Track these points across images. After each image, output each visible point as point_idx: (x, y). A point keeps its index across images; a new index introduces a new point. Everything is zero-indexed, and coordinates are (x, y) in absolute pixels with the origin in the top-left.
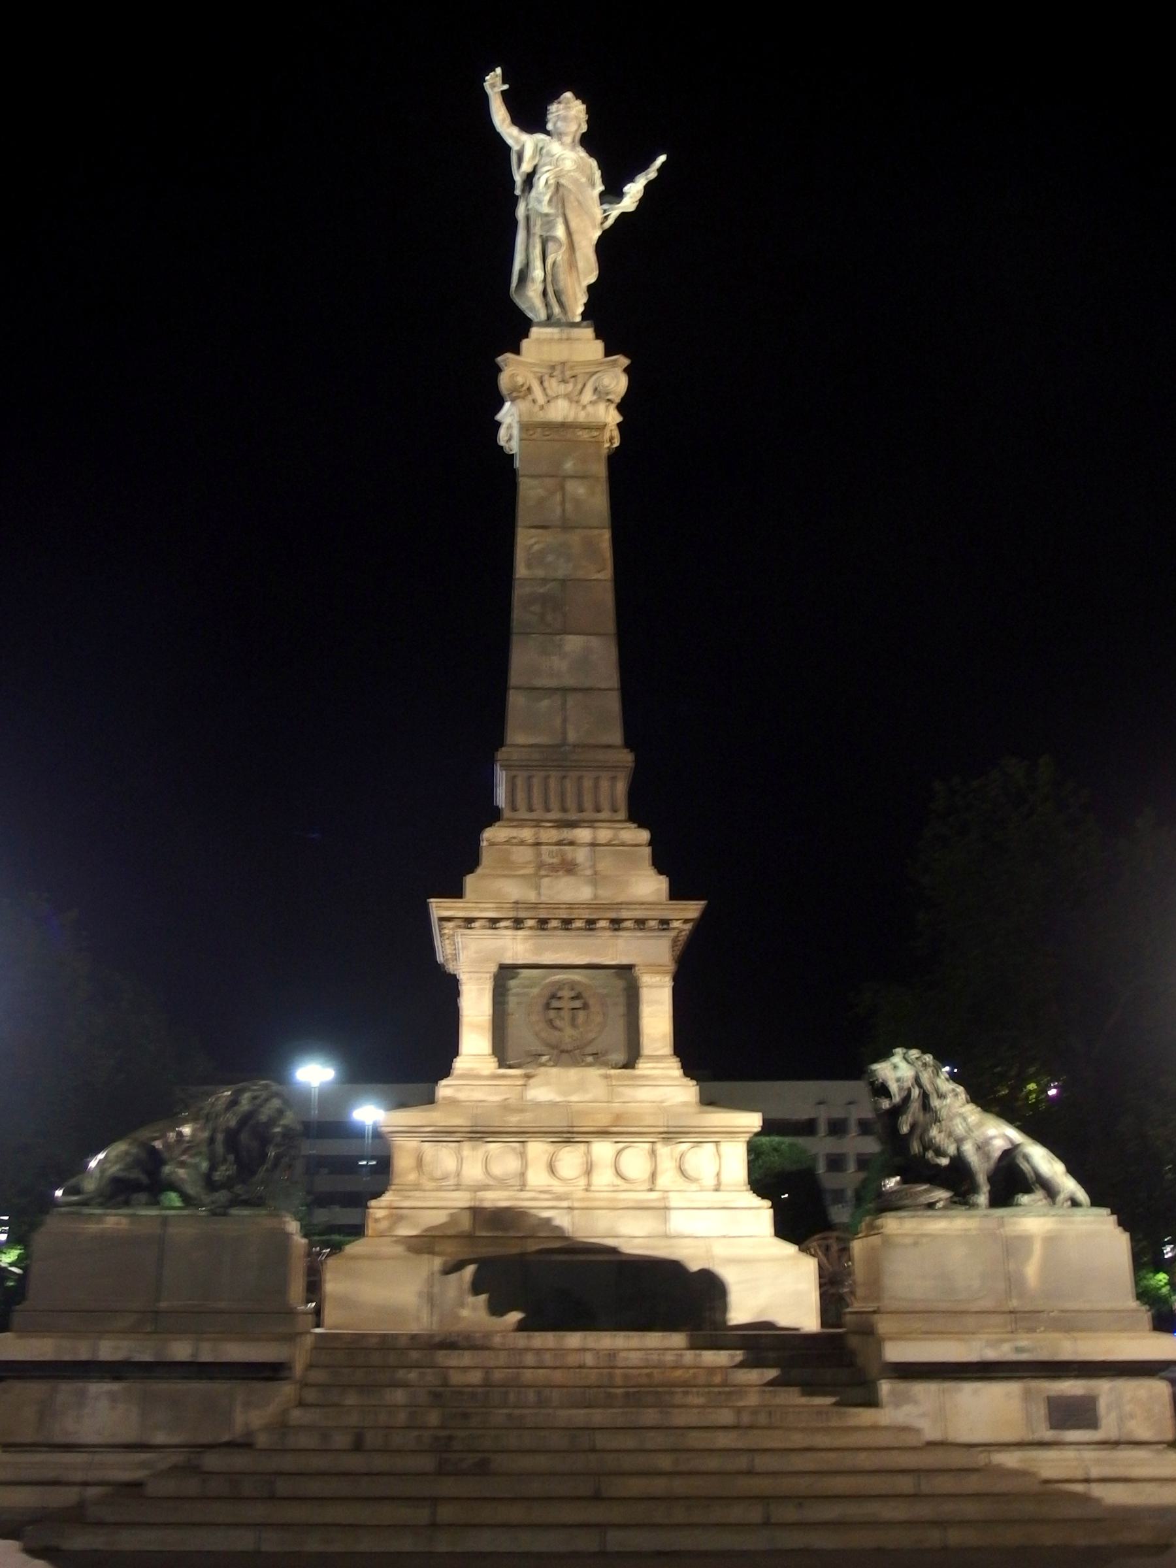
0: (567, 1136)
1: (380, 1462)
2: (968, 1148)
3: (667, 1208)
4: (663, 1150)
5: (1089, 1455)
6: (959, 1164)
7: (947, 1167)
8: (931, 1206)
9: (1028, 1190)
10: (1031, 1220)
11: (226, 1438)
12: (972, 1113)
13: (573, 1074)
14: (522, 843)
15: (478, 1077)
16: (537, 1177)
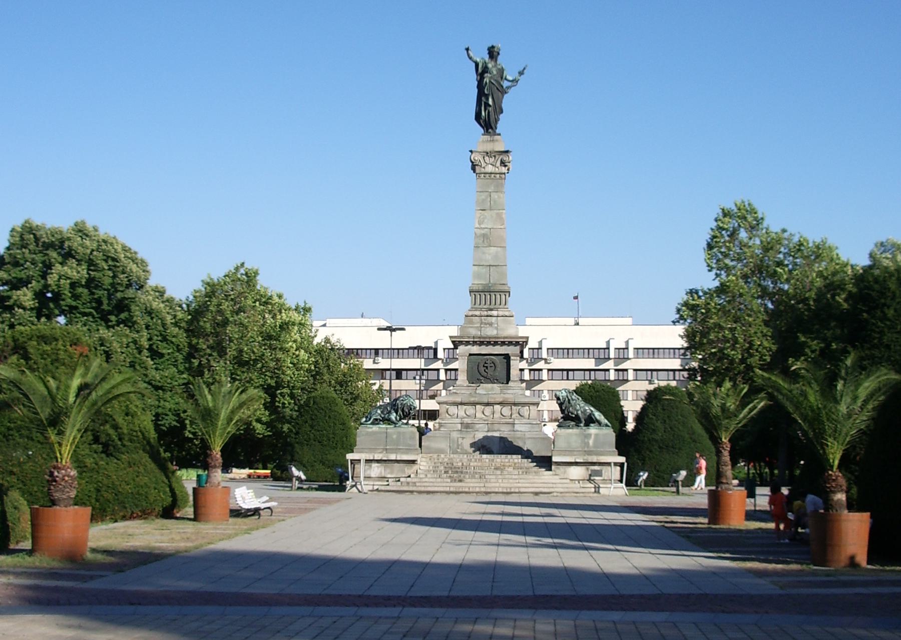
0: (488, 404)
6: (577, 416)
9: (594, 422)
10: (593, 430)
12: (582, 404)
13: (490, 385)
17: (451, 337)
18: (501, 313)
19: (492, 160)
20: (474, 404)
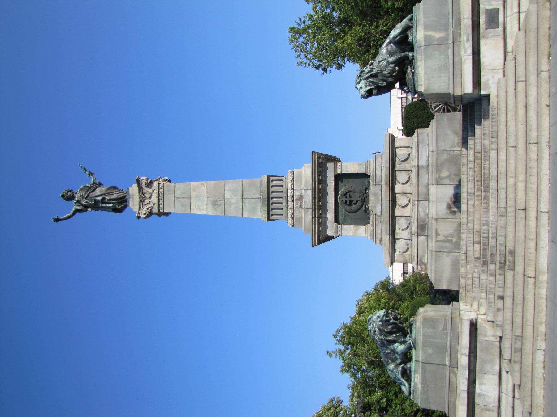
1: (509, 292)
2: (391, 60)
3: (418, 166)
4: (398, 167)
5: (508, 12)
7: (399, 67)
8: (413, 73)
9: (407, 37)
10: (419, 35)
11: (498, 344)
12: (379, 58)
13: (372, 198)
14: (293, 214)
15: (373, 231)
16: (407, 211)
17: (314, 245)
18: (290, 185)
19: (147, 196)
20: (393, 218)
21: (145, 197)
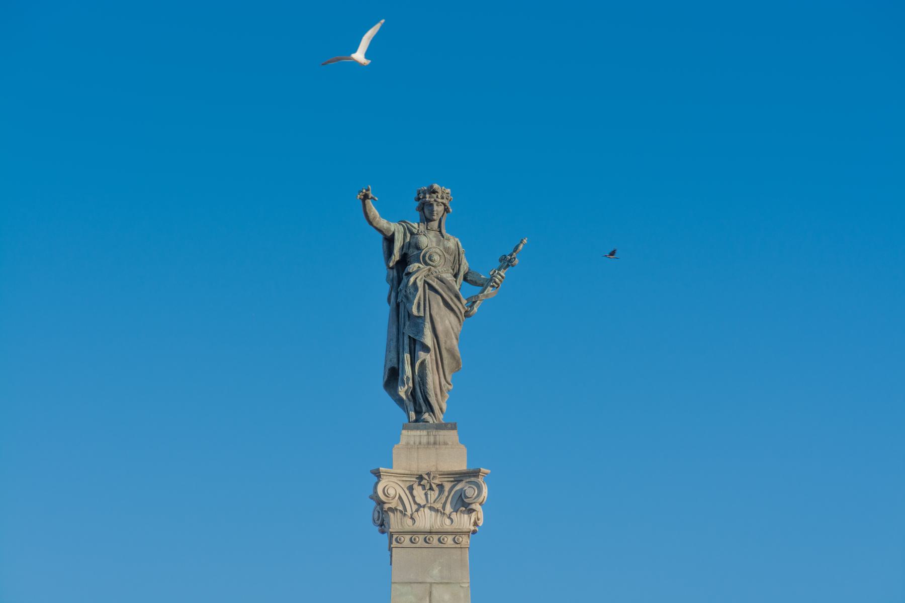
21: (431, 489)
